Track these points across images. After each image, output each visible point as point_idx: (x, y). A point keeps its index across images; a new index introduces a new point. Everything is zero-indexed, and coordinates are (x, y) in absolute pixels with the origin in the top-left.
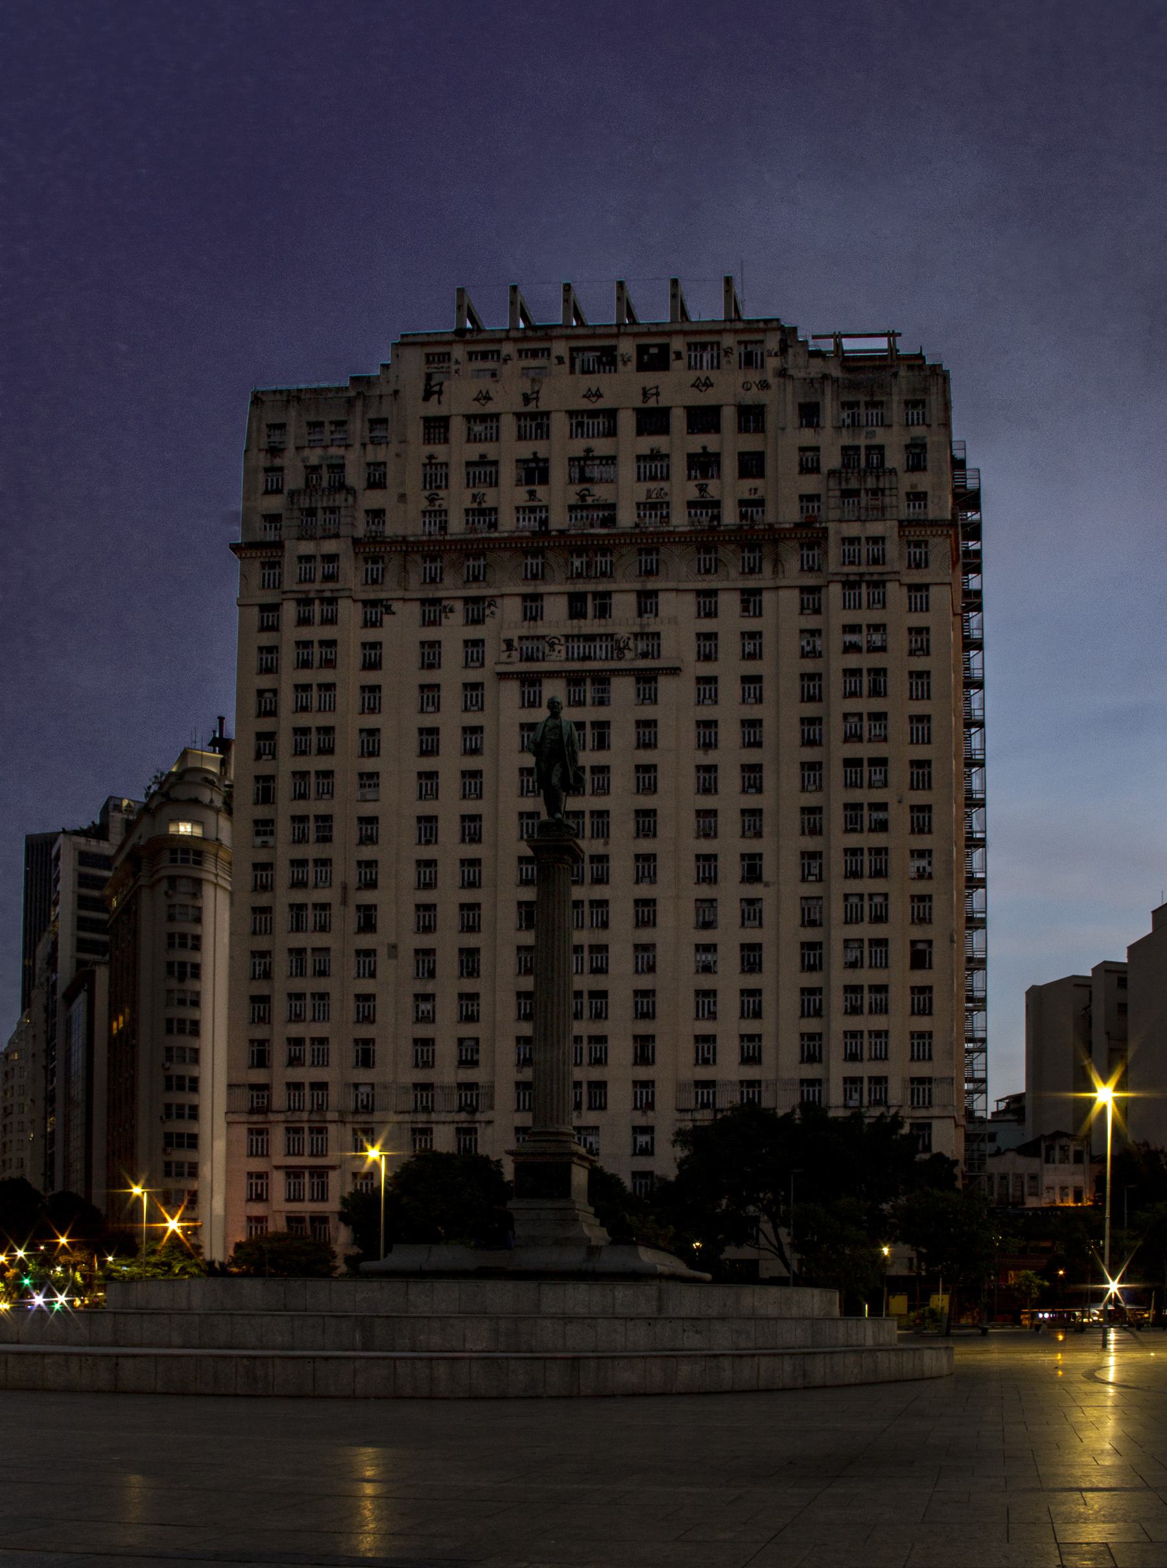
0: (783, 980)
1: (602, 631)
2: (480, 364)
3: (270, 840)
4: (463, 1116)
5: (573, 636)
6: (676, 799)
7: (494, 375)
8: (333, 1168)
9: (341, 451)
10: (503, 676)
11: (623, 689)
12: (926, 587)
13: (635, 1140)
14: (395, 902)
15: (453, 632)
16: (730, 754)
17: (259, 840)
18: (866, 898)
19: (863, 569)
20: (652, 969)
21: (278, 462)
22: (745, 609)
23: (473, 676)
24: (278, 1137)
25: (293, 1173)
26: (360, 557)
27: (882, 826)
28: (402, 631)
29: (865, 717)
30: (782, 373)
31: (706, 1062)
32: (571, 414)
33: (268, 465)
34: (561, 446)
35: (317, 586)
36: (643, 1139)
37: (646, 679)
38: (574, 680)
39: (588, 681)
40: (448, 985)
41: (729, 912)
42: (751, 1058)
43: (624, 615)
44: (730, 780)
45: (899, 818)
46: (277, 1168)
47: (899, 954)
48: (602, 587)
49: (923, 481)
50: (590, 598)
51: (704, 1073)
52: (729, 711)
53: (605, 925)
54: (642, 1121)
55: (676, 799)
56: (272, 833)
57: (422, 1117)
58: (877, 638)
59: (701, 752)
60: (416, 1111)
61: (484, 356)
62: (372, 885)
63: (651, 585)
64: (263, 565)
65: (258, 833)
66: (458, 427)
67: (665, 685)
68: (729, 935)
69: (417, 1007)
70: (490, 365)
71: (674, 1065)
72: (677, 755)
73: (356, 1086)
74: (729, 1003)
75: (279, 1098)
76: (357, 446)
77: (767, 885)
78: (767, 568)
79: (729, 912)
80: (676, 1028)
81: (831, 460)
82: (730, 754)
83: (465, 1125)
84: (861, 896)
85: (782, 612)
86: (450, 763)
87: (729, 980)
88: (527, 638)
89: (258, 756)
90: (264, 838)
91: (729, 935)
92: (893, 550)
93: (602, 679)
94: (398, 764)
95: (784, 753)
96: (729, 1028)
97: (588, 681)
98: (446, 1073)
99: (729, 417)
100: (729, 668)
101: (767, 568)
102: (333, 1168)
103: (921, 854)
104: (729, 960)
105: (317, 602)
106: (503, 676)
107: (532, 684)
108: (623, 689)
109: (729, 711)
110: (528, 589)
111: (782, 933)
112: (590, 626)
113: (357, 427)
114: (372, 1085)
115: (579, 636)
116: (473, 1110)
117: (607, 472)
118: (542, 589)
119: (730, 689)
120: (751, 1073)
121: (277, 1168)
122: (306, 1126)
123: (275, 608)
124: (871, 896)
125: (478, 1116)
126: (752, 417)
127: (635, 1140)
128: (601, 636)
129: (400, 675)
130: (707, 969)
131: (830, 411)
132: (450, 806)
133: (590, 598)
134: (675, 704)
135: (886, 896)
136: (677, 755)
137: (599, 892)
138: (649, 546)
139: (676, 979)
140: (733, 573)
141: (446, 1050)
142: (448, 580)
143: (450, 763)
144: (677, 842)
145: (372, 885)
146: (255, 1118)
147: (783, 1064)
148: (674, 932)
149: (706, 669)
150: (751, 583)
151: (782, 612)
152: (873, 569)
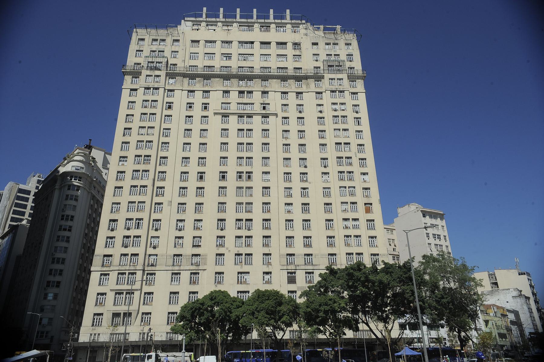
0: (317, 215)
1: (250, 102)
2: (210, 27)
3: (125, 163)
4: (194, 267)
5: (240, 104)
6: (276, 153)
7: (215, 30)
8: (137, 290)
9: (164, 47)
10: (215, 114)
11: (257, 119)
12: (357, 93)
13: (264, 277)
14: (171, 185)
15: (198, 99)
16: (294, 139)
17: (121, 163)
18: (347, 187)
19: (337, 87)
20: (269, 211)
21: (141, 49)
22: (297, 98)
23: (205, 113)
24: (113, 276)
25: (119, 293)
26: (168, 78)
27: (351, 164)
28: (180, 99)
29: (341, 130)
30: (306, 35)
31: (290, 246)
32: (240, 42)
33: (138, 49)
34: (234, 49)
35: (153, 84)
36: (267, 277)
37: (265, 116)
38: (241, 116)
39: (245, 117)
40: (190, 216)
41: (296, 192)
42: (308, 245)
43: (257, 97)
44: (294, 148)
45: (355, 161)
46: (111, 290)
47: (361, 207)
48: (250, 89)
49: (352, 64)
50: (246, 92)
51: (290, 251)
52: (293, 126)
53: (251, 195)
54: (267, 270)
55: (276, 153)
56: (126, 161)
57: (177, 268)
58: (343, 107)
59: (284, 140)
60: (173, 265)
61: (211, 25)
62: (164, 179)
63: (266, 90)
64: (133, 77)
65: (120, 161)
66: (202, 43)
67: (271, 119)
68: (297, 200)
69: (177, 224)
70: (214, 27)
71: (278, 248)
72: (276, 139)
73: (150, 255)
74: (298, 224)
75: (116, 260)
76: (169, 46)
77: (310, 183)
78: (304, 86)
79: (296, 192)
80: (278, 232)
81: (323, 57)
82: (294, 139)
83: (194, 271)
84: (345, 187)
85: (309, 99)
86: (195, 139)
87: (298, 216)
88: (224, 103)
89: (124, 135)
90: (123, 163)
91: (297, 200)
92: (346, 83)
93: (250, 116)
94: (176, 139)
95: (312, 140)
96: (298, 233)
97: (245, 117)
98: (188, 250)
99: (289, 45)
100: (293, 114)
101: (304, 86)
102: (137, 290)
103: (364, 174)
104: (297, 208)
105: (152, 89)
106: (215, 114)
107: (226, 117)
108: (257, 119)
109: (293, 126)
110: (225, 89)
111: (316, 200)
112: (245, 100)
113: (169, 40)
114: (157, 255)
115: (242, 104)
116: (197, 265)
117: (250, 58)
118: (229, 89)
119: (293, 120)
120: (308, 251)
121: (111, 290)
122: (127, 272)
123: (136, 90)
124: (349, 187)
125: (200, 268)
126: (296, 45)
127: (264, 277)
128: (249, 104)
129: (179, 111)
130: (289, 212)
131: (322, 44)
132: (194, 154)
133: (246, 92)
134: (274, 124)
135: (354, 187)
136: (276, 139)
137: (249, 184)
138: (265, 78)
139: (278, 214)
140: (293, 87)
141: (188, 241)
142: (197, 85)
143: (195, 139)
144: (276, 167)
145: (164, 179)
146: (105, 269)
147: (320, 247)
148: (277, 198)
149: (285, 115)
150: (299, 90)
151: (309, 99)
152: (340, 87)
